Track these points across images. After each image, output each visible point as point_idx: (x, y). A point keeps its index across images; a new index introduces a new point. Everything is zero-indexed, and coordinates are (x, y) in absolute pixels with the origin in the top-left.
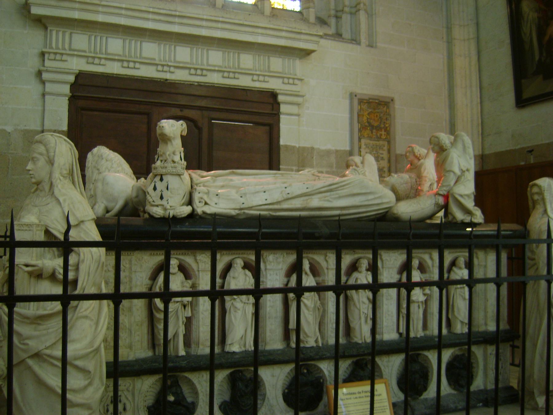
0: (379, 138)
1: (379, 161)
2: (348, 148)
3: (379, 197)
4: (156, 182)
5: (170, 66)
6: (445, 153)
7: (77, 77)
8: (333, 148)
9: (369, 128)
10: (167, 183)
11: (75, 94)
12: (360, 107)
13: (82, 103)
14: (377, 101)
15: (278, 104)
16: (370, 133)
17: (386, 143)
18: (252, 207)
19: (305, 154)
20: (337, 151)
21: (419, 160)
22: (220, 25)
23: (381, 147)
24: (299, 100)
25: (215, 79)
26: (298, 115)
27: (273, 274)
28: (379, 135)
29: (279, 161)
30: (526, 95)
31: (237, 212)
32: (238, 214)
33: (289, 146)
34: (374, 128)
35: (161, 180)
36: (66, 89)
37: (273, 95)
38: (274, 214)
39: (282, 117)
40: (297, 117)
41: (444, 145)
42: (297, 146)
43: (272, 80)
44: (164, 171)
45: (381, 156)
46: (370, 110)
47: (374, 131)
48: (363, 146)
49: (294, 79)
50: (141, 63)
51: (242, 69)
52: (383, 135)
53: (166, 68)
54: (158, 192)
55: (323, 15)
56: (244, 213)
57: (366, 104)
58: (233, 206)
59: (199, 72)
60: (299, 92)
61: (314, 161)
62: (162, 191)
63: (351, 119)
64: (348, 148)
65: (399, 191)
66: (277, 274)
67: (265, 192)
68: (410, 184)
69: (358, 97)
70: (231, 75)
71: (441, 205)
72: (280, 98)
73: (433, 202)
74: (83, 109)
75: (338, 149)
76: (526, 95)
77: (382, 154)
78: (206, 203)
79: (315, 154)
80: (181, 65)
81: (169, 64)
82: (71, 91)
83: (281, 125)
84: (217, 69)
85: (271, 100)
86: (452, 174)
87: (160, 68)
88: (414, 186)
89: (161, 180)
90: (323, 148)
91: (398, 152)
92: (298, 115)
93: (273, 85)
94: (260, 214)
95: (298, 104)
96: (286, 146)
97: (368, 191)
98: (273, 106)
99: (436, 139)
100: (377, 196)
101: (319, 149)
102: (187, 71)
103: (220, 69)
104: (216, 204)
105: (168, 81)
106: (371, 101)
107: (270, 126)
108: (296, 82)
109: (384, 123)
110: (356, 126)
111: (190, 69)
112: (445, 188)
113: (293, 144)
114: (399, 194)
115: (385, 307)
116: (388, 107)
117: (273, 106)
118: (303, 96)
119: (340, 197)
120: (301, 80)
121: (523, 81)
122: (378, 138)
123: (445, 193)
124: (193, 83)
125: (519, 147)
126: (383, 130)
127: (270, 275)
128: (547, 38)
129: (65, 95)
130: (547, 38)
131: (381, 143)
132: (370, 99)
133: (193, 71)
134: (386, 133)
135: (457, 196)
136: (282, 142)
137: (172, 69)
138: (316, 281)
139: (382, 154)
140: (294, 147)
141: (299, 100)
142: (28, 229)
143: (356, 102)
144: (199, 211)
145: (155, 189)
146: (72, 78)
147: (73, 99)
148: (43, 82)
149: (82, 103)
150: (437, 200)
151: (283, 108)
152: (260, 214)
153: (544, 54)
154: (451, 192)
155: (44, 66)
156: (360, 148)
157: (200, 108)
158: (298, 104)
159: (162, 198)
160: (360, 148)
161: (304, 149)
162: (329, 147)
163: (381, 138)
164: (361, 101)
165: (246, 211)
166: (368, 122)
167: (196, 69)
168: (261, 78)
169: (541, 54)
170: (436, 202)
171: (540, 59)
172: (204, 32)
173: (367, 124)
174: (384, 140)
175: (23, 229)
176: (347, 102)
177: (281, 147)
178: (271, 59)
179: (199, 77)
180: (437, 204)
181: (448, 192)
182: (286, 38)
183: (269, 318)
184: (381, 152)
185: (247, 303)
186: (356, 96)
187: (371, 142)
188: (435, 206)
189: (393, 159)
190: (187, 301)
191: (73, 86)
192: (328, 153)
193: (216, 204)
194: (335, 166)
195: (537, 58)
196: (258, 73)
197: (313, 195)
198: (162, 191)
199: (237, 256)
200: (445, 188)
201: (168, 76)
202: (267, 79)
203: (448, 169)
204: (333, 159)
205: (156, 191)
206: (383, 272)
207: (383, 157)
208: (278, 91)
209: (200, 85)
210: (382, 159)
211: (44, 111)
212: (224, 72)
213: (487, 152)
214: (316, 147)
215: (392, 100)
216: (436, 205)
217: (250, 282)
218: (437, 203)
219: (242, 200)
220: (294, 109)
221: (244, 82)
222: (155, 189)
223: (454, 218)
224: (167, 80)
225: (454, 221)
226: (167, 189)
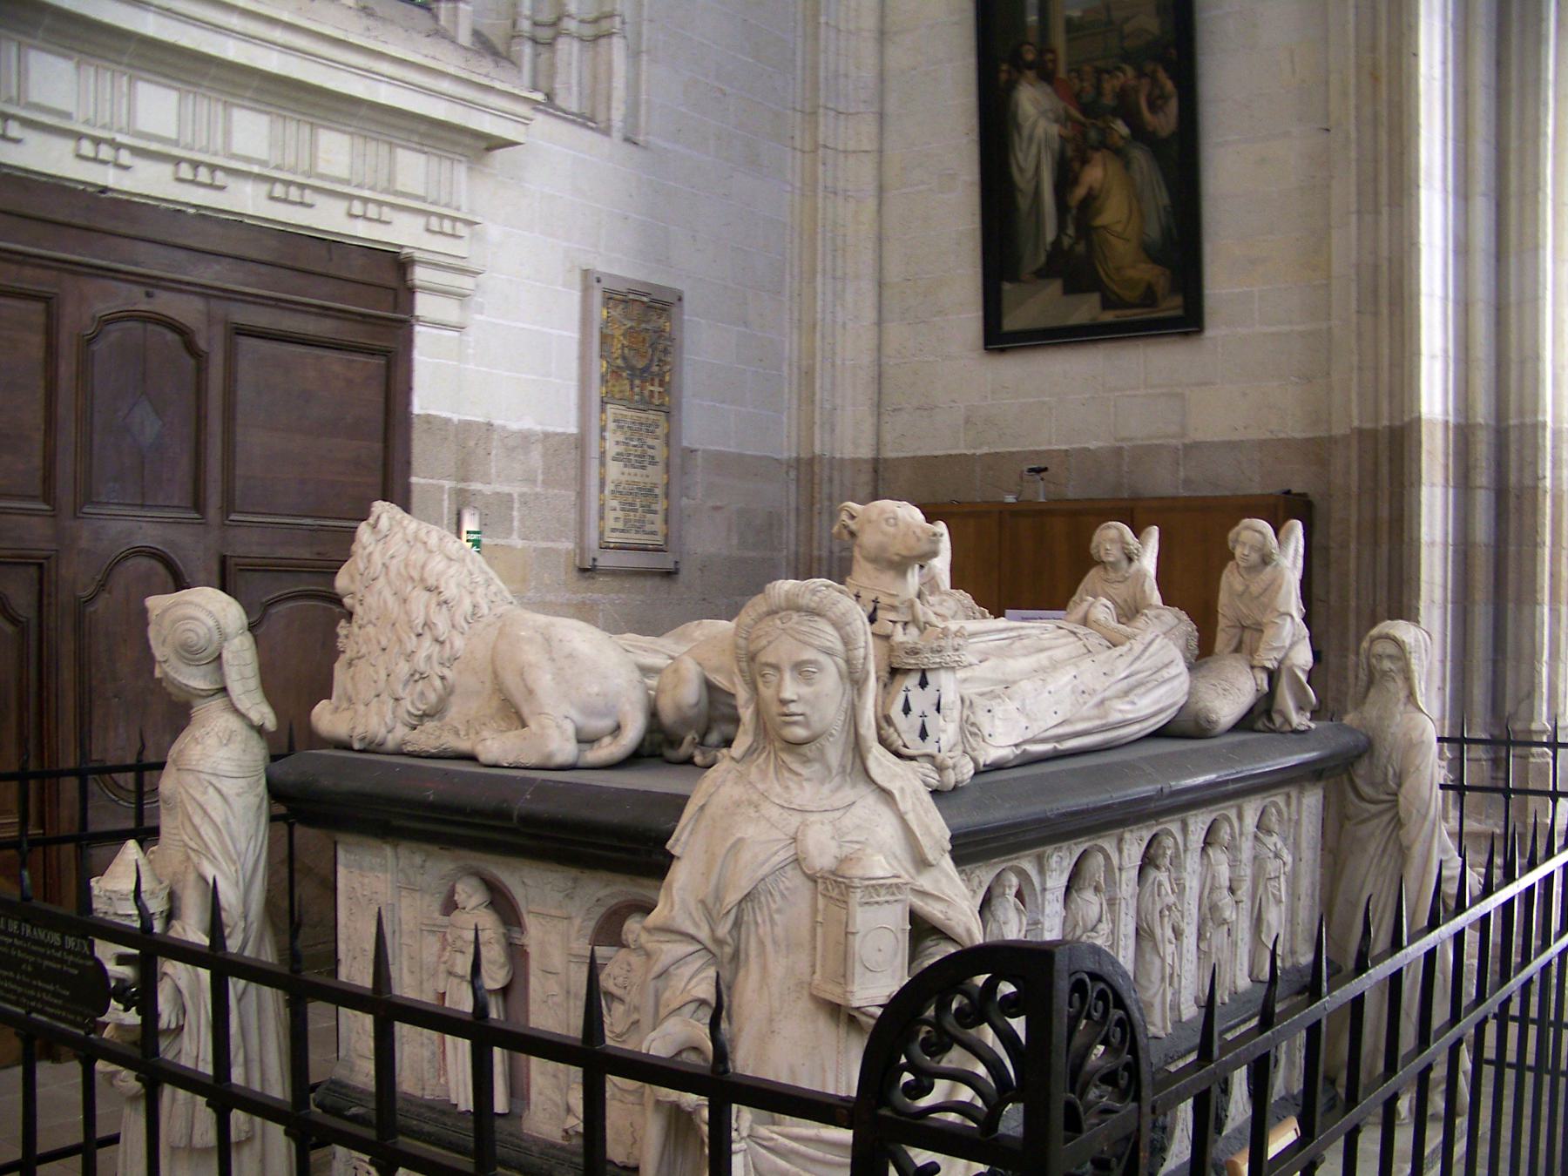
0: (646, 404)
1: (643, 468)
2: (573, 429)
5: (117, 146)
8: (538, 428)
9: (624, 374)
14: (645, 299)
15: (411, 291)
16: (628, 387)
17: (661, 418)
19: (472, 443)
20: (547, 435)
22: (278, 35)
23: (650, 428)
25: (247, 200)
26: (459, 328)
28: (646, 393)
29: (408, 463)
30: (1011, 323)
33: (435, 417)
34: (638, 372)
35: (923, 684)
37: (397, 265)
39: (419, 329)
42: (455, 417)
43: (402, 220)
45: (651, 452)
46: (629, 324)
47: (637, 382)
48: (611, 425)
49: (455, 219)
50: (137, 152)
51: (322, 177)
52: (656, 395)
53: (105, 152)
54: (914, 720)
55: (496, 30)
56: (1025, 750)
57: (621, 306)
59: (204, 175)
61: (493, 464)
62: (923, 715)
63: (584, 343)
64: (573, 429)
69: (605, 284)
70: (294, 194)
72: (420, 275)
75: (551, 429)
76: (1011, 323)
77: (652, 447)
79: (495, 444)
80: (154, 146)
81: (120, 138)
84: (256, 169)
85: (390, 279)
86: (1289, 619)
87: (87, 148)
89: (923, 684)
90: (514, 426)
91: (685, 443)
92: (459, 328)
93: (402, 233)
95: (460, 296)
96: (428, 419)
98: (396, 297)
101: (504, 428)
102: (167, 169)
103: (266, 172)
105: (109, 194)
106: (631, 296)
107: (385, 353)
108: (461, 229)
109: (660, 360)
110: (598, 367)
111: (177, 161)
113: (445, 414)
116: (669, 319)
117: (396, 297)
121: (1007, 286)
122: (642, 401)
124: (183, 208)
125: (985, 450)
126: (657, 381)
128: (1080, 192)
130: (1080, 192)
131: (651, 416)
132: (630, 291)
133: (186, 171)
134: (661, 390)
136: (419, 406)
137: (125, 157)
139: (652, 447)
140: (447, 421)
141: (465, 282)
142: (891, 898)
143: (597, 297)
145: (907, 709)
151: (424, 305)
153: (1071, 231)
156: (603, 429)
157: (207, 292)
158: (460, 296)
159: (923, 734)
160: (603, 429)
161: (467, 426)
162: (529, 423)
163: (651, 403)
164: (610, 298)
166: (624, 358)
167: (196, 165)
168: (372, 211)
169: (1061, 227)
171: (1057, 243)
172: (233, 51)
173: (620, 362)
174: (659, 408)
175: (877, 899)
176: (576, 296)
177: (415, 420)
178: (400, 152)
179: (202, 191)
181: (1280, 662)
182: (452, 98)
184: (650, 442)
186: (599, 281)
187: (629, 413)
189: (676, 461)
192: (526, 438)
194: (540, 478)
195: (1050, 235)
196: (366, 193)
198: (923, 715)
199: (1004, 866)
202: (387, 213)
203: (1282, 610)
204: (536, 457)
207: (653, 457)
208: (417, 255)
209: (206, 217)
210: (653, 462)
212: (273, 180)
213: (889, 453)
214: (497, 422)
215: (680, 299)
221: (328, 218)
222: (907, 709)
223: (1287, 721)
224: (104, 190)
226: (938, 710)
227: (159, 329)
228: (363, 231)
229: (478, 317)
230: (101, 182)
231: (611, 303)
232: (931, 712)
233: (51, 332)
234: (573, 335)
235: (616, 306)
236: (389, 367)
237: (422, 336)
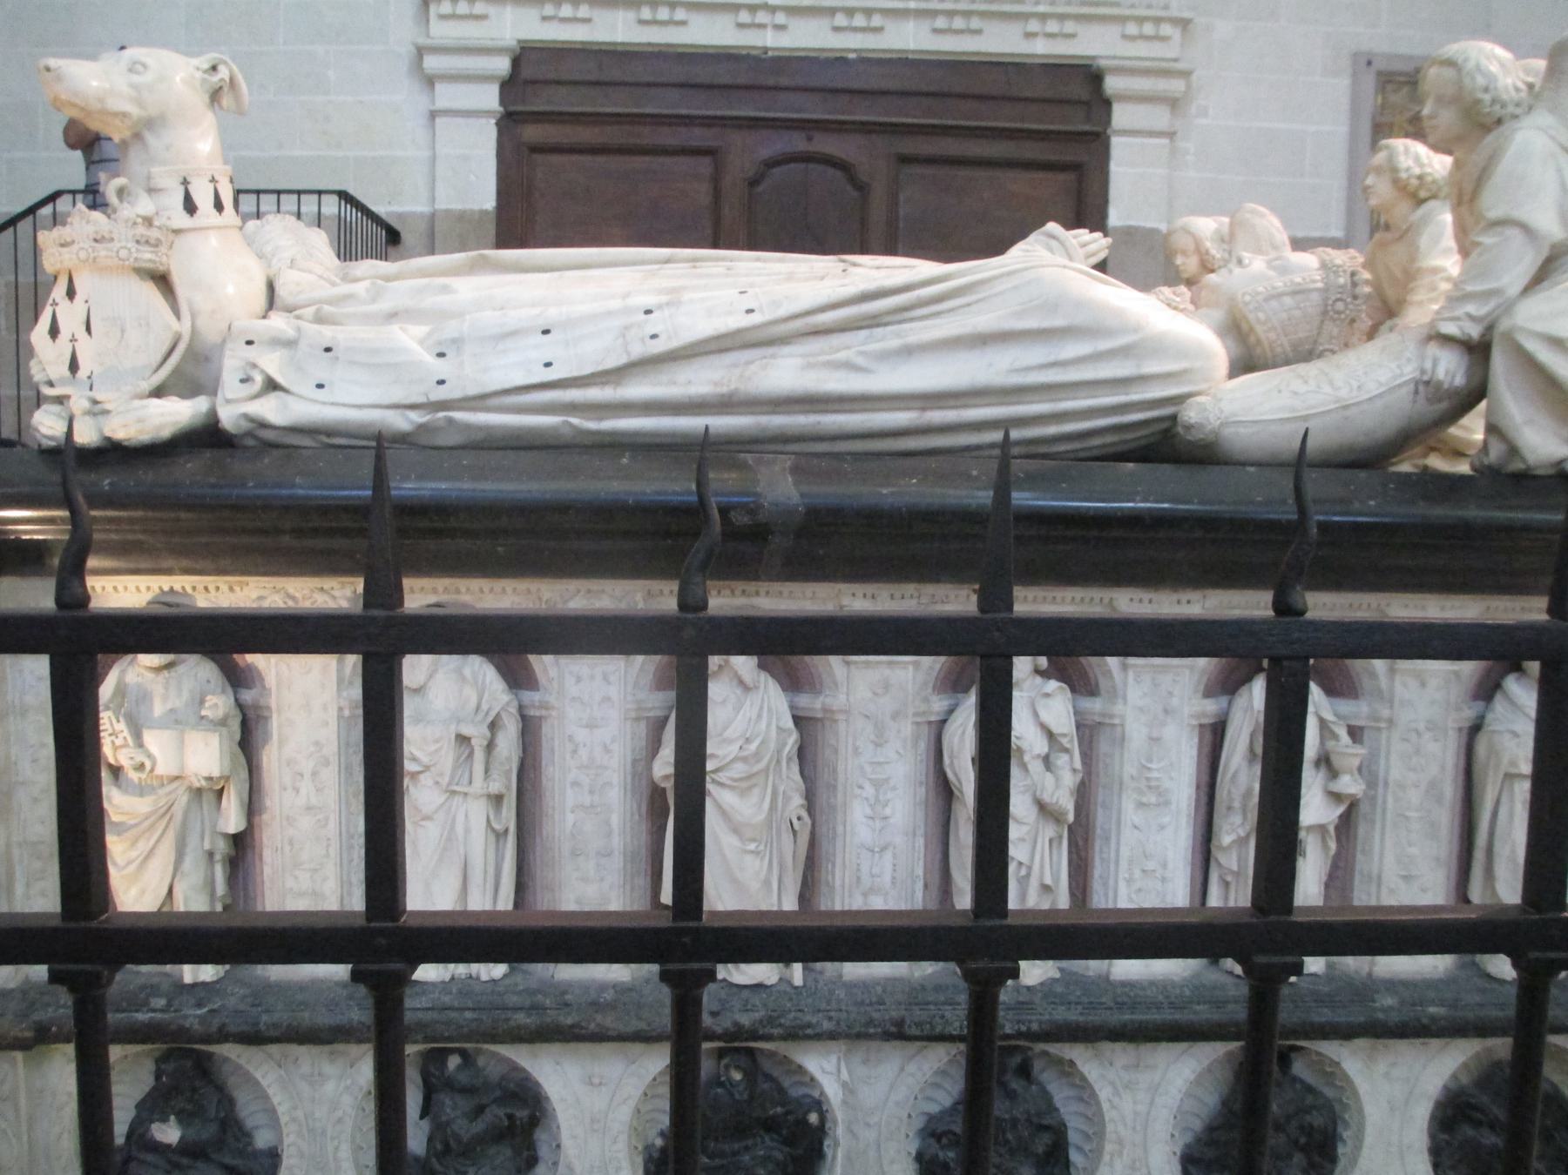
3: (1124, 352)
4: (57, 304)
6: (1490, 138)
7: (516, 62)
10: (86, 306)
11: (512, 108)
12: (1384, 98)
13: (532, 133)
15: (1107, 104)
18: (484, 397)
21: (1420, 202)
24: (1176, 86)
26: (1171, 135)
27: (592, 677)
31: (417, 417)
32: (422, 427)
33: (1137, 229)
36: (489, 98)
37: (1090, 76)
38: (592, 425)
39: (1116, 142)
40: (1165, 141)
41: (1487, 97)
44: (148, 256)
54: (63, 346)
56: (450, 421)
58: (399, 395)
60: (1176, 60)
62: (74, 339)
65: (1259, 329)
66: (605, 678)
67: (546, 332)
68: (1315, 297)
69: (1379, 65)
71: (1446, 386)
72: (1112, 84)
73: (1409, 371)
74: (536, 149)
78: (272, 386)
82: (502, 102)
83: (1114, 167)
88: (1340, 306)
92: (1171, 135)
94: (707, 428)
97: (1058, 322)
99: (1448, 73)
100: (1104, 345)
104: (320, 386)
105: (770, 54)
107: (1076, 167)
108: (1166, 29)
112: (1471, 308)
113: (1149, 225)
114: (1259, 342)
115: (1128, 836)
118: (1185, 74)
119: (908, 352)
120: (1184, 24)
123: (1474, 332)
124: (844, 55)
127: (579, 680)
129: (487, 113)
135: (1532, 346)
137: (780, 18)
138: (792, 707)
141: (1176, 86)
143: (1369, 82)
144: (228, 417)
145: (54, 331)
146: (502, 65)
147: (509, 121)
148: (430, 81)
149: (532, 133)
150: (1428, 365)
151: (1121, 116)
152: (707, 428)
154: (1504, 325)
155: (428, 36)
157: (866, 128)
158: (1174, 103)
165: (458, 415)
170: (1423, 372)
179: (859, 36)
180: (1427, 383)
181: (1490, 328)
183: (575, 854)
185: (466, 794)
186: (1369, 63)
188: (1416, 392)
190: (207, 775)
191: (510, 86)
193: (320, 386)
197: (784, 340)
198: (74, 339)
200: (1471, 308)
201: (770, 40)
203: (1493, 214)
205: (57, 341)
206: (1125, 684)
208: (1103, 63)
211: (433, 159)
216: (1421, 388)
217: (485, 707)
218: (1426, 378)
219: (442, 368)
220: (1159, 117)
222: (54, 331)
225: (1517, 466)
226: (88, 329)
227: (820, 168)
228: (1041, 48)
229: (1203, 121)
230: (760, 44)
231: (1389, 87)
232: (81, 333)
233: (716, 180)
234: (1343, 129)
235: (1395, 91)
236: (1080, 181)
237: (1120, 148)
